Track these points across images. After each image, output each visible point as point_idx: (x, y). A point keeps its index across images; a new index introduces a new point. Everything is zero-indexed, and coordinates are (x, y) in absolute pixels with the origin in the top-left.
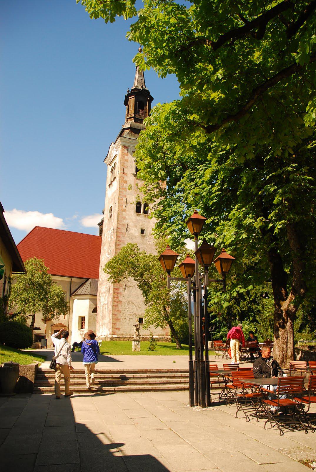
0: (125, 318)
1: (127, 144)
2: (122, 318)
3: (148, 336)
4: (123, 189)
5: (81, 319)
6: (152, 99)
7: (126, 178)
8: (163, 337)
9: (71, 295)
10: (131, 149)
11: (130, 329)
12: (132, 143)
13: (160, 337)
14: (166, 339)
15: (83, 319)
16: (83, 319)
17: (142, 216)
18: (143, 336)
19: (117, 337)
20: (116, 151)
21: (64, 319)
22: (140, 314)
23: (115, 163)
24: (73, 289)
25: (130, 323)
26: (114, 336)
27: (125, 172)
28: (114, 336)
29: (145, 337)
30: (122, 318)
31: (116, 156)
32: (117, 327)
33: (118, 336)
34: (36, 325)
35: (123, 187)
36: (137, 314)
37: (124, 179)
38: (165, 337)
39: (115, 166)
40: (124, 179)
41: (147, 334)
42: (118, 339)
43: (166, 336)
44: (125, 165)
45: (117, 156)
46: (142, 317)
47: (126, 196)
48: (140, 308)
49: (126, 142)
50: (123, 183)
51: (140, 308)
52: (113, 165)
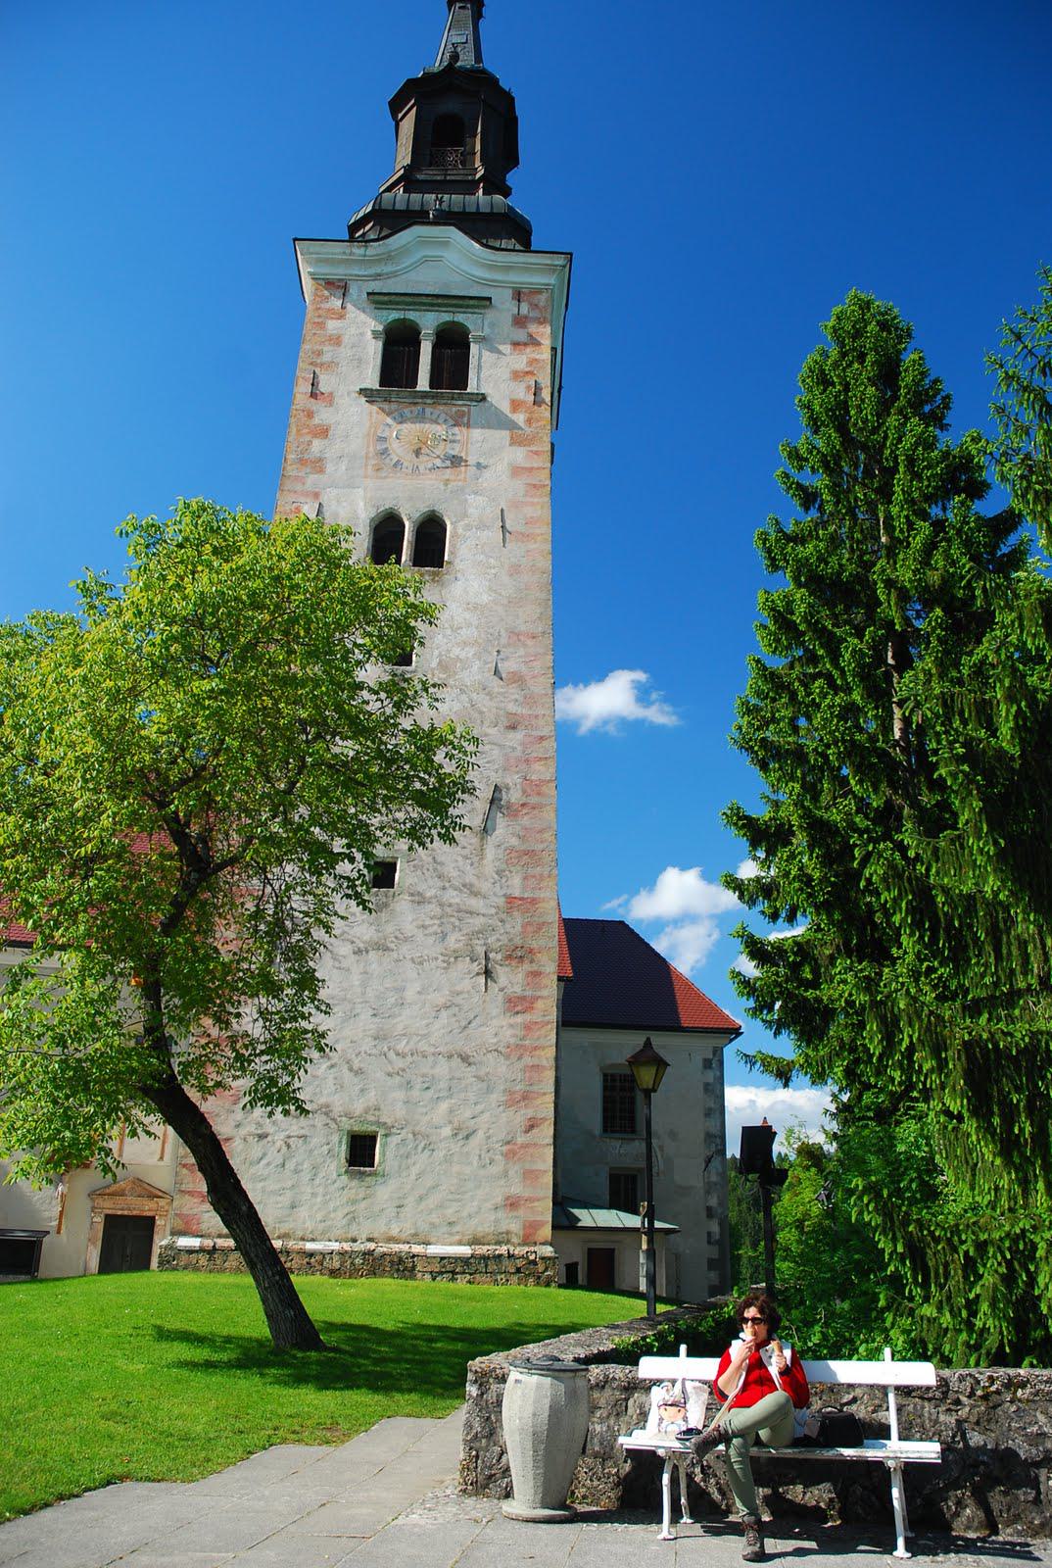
0: (262, 1137)
1: (338, 272)
2: (243, 1132)
3: (405, 1248)
4: (302, 462)
7: (324, 415)
8: (503, 1250)
10: (360, 291)
11: (286, 1199)
12: (363, 262)
13: (482, 1250)
14: (520, 1263)
18: (371, 1246)
19: (202, 1250)
21: (161, 1158)
22: (358, 1107)
25: (290, 1165)
26: (184, 1242)
27: (323, 387)
28: (184, 1242)
29: (383, 1248)
30: (243, 1132)
33: (208, 1243)
35: (306, 456)
36: (337, 1109)
37: (316, 421)
38: (519, 1251)
40: (316, 421)
41: (395, 1232)
42: (203, 1260)
43: (525, 1243)
44: (326, 358)
46: (374, 1128)
47: (316, 495)
48: (359, 1072)
49: (327, 261)
50: (308, 438)
51: (359, 1072)
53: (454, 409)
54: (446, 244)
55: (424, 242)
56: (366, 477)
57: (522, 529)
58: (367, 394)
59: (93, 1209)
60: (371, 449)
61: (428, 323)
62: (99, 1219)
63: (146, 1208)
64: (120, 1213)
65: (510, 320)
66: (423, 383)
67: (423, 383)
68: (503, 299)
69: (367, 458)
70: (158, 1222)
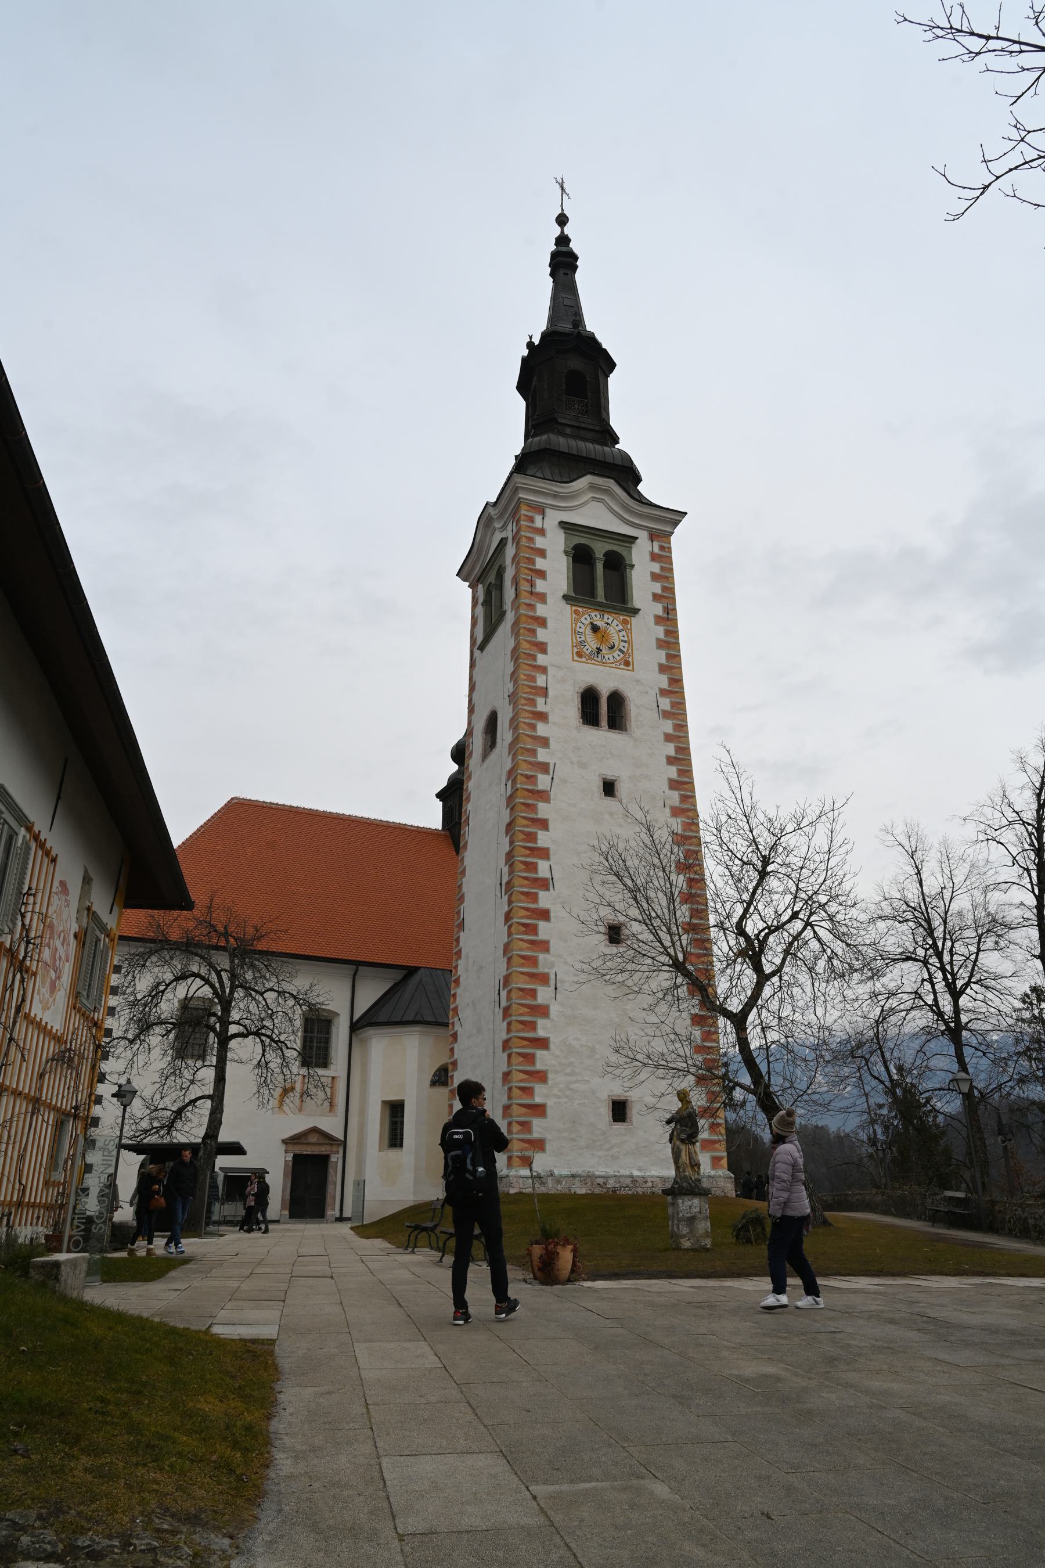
5: (388, 1113)
6: (611, 365)
9: (355, 1027)
15: (395, 1110)
16: (395, 1110)
17: (601, 736)
20: (504, 528)
23: (501, 566)
24: (363, 1006)
31: (503, 542)
32: (535, 1135)
34: (224, 1136)
39: (500, 575)
45: (505, 544)
52: (492, 578)
53: (622, 617)
54: (607, 491)
55: (593, 487)
56: (573, 660)
57: (668, 708)
58: (566, 597)
59: (286, 1151)
60: (575, 641)
61: (600, 549)
62: (290, 1157)
63: (323, 1150)
64: (305, 1153)
65: (648, 557)
66: (600, 596)
67: (600, 596)
68: (643, 536)
69: (573, 646)
70: (332, 1160)
